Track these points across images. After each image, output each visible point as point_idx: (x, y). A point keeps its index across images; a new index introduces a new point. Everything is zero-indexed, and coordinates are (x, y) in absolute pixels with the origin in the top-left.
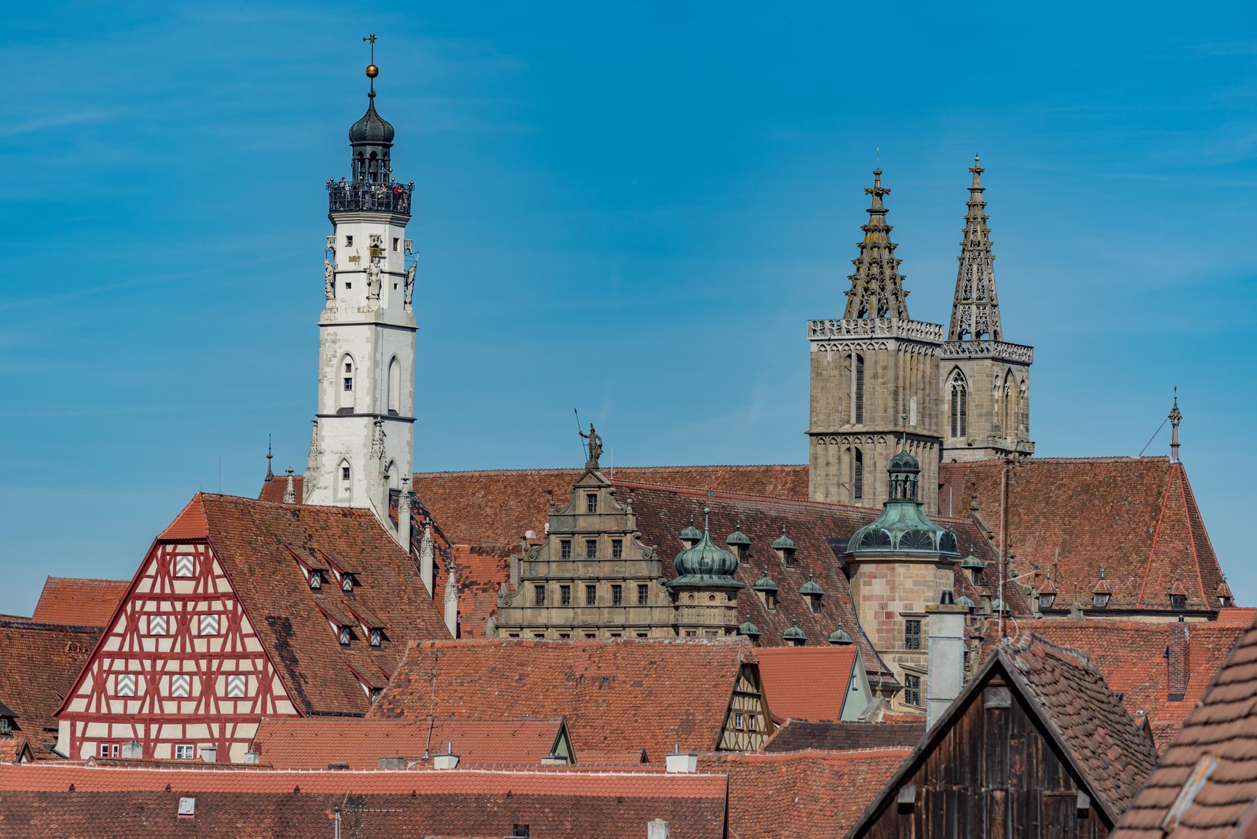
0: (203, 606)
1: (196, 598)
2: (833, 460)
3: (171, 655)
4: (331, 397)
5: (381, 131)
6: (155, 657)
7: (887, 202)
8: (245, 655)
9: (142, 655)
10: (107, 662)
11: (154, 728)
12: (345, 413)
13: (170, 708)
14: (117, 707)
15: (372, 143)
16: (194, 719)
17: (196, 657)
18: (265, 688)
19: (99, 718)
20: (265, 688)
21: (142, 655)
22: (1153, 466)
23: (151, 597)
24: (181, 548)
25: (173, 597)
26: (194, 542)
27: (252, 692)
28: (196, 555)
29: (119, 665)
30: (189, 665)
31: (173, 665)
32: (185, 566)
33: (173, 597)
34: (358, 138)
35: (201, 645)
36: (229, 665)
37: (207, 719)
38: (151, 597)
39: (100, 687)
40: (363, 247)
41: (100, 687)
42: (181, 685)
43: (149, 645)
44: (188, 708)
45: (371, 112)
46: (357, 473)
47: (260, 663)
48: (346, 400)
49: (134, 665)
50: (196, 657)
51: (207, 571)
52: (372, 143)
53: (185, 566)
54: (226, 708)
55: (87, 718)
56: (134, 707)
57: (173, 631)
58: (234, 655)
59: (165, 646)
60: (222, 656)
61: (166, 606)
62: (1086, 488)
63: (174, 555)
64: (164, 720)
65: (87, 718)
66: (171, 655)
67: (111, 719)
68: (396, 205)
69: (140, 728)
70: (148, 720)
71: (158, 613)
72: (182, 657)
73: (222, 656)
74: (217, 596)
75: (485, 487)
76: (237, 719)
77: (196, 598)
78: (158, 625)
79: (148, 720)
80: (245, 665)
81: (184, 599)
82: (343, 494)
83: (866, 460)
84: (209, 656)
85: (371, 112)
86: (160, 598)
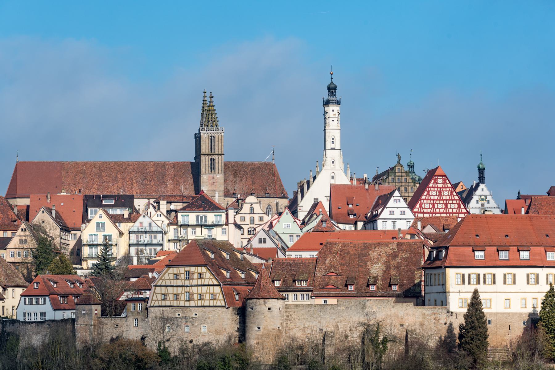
0: (444, 189)
1: (443, 188)
2: (207, 161)
3: (437, 200)
4: (329, 145)
5: (333, 86)
6: (433, 200)
7: (213, 100)
8: (454, 200)
9: (431, 200)
10: (422, 201)
11: (434, 215)
12: (332, 149)
13: (438, 211)
14: (425, 210)
15: (332, 89)
16: (443, 213)
17: (443, 200)
18: (459, 206)
19: (421, 213)
20: (459, 206)
21: (431, 200)
22: (268, 164)
23: (432, 187)
24: (439, 177)
25: (438, 188)
26: (442, 176)
27: (456, 207)
28: (443, 179)
29: (425, 201)
30: (442, 202)
31: (438, 202)
32: (440, 181)
33: (438, 188)
34: (329, 88)
35: (444, 198)
36: (451, 202)
37: (446, 213)
38: (432, 187)
39: (421, 206)
40: (336, 112)
41: (421, 206)
42: (440, 206)
43: (432, 198)
44: (442, 211)
45: (332, 83)
46: (337, 162)
47: (458, 201)
48: (333, 146)
49: (429, 201)
50: (443, 200)
51: (445, 182)
52: (332, 89)
53: (440, 181)
54: (451, 211)
55: (418, 213)
56: (429, 211)
57: (438, 194)
58: (452, 200)
59: (436, 197)
60: (449, 200)
61: (436, 189)
62: (253, 169)
63: (437, 179)
64: (436, 213)
65: (418, 213)
66: (437, 200)
67: (424, 213)
68: (338, 103)
69: (431, 215)
70: (432, 213)
71: (434, 191)
72: (440, 200)
73: (449, 200)
74: (448, 187)
75: (85, 165)
76: (453, 213)
77: (443, 188)
78: (434, 193)
79: (432, 213)
80: (455, 202)
81: (440, 188)
82: (332, 167)
83: (216, 161)
84: (446, 200)
85: (332, 83)
86: (434, 188)
